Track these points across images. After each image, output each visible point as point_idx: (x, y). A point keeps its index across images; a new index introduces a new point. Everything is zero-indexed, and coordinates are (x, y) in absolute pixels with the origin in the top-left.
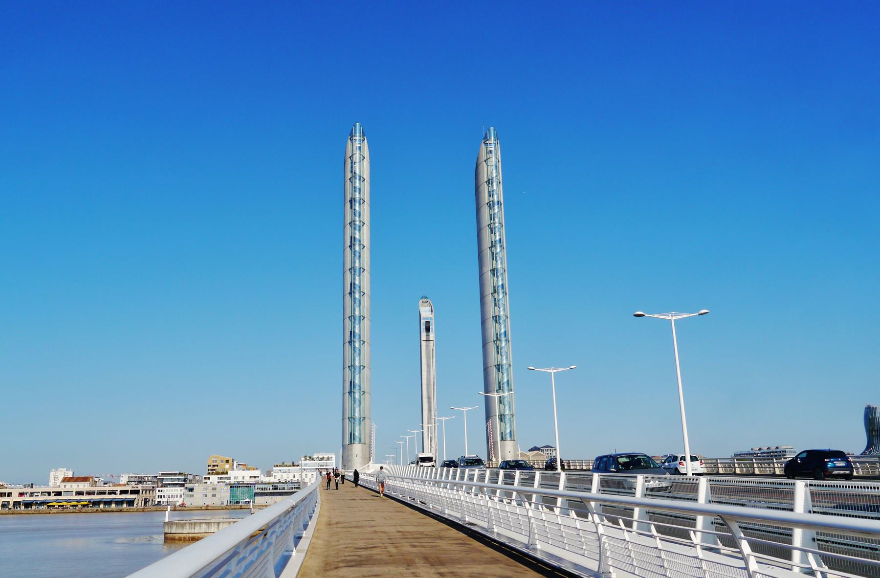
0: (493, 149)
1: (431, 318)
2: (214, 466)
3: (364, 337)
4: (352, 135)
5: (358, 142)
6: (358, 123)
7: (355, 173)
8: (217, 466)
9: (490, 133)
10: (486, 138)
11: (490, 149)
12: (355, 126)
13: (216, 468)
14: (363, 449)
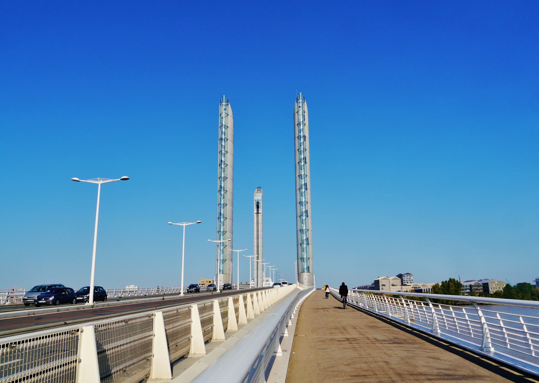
0: (301, 105)
1: (260, 200)
2: (202, 284)
3: (227, 215)
4: (221, 102)
5: (224, 106)
6: (224, 96)
7: (222, 124)
8: (204, 284)
9: (299, 96)
10: (297, 100)
11: (299, 105)
12: (222, 97)
13: (204, 285)
14: (224, 277)
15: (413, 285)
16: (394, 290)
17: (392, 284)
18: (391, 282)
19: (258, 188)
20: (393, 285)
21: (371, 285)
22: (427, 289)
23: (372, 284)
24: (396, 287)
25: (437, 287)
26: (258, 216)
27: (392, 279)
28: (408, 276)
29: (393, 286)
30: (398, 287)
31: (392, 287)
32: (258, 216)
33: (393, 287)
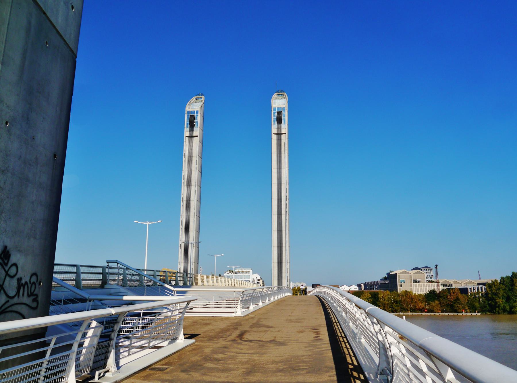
15: (442, 281)
16: (416, 288)
17: (415, 279)
18: (412, 278)
20: (415, 281)
21: (380, 280)
22: (471, 288)
23: (381, 280)
24: (419, 283)
25: (495, 285)
26: (191, 143)
27: (414, 274)
28: (429, 270)
29: (415, 282)
30: (422, 283)
31: (414, 283)
32: (192, 142)
33: (416, 283)
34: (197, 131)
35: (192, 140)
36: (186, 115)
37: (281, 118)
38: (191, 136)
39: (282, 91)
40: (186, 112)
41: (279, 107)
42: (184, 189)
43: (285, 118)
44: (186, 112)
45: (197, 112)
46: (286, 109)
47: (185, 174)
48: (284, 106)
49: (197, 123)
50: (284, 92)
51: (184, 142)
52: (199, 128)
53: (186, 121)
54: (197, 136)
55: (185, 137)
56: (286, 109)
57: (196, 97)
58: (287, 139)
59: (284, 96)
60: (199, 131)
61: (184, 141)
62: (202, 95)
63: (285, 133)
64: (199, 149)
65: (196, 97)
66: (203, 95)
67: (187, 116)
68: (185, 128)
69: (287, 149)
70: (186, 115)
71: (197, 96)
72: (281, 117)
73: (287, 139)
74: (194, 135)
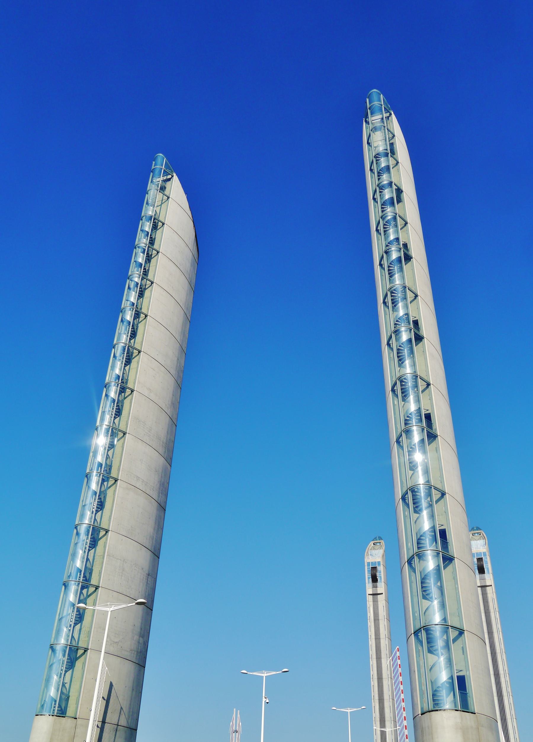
19: (375, 539)
26: (375, 602)
32: (377, 601)
34: (381, 587)
35: (377, 598)
36: (366, 567)
37: (483, 566)
38: (375, 595)
39: (478, 529)
40: (366, 564)
41: (478, 552)
42: (373, 662)
43: (488, 566)
44: (366, 564)
45: (379, 563)
46: (487, 554)
47: (372, 642)
48: (485, 550)
49: (381, 577)
50: (481, 530)
51: (368, 602)
52: (383, 584)
53: (368, 576)
54: (382, 594)
55: (367, 595)
56: (487, 554)
57: (374, 542)
58: (494, 593)
59: (481, 535)
60: (384, 588)
61: (368, 600)
62: (380, 538)
63: (491, 585)
64: (386, 610)
65: (374, 542)
66: (382, 540)
67: (368, 568)
68: (367, 584)
69: (496, 606)
70: (366, 567)
71: (373, 540)
72: (483, 564)
73: (494, 593)
74: (378, 593)
